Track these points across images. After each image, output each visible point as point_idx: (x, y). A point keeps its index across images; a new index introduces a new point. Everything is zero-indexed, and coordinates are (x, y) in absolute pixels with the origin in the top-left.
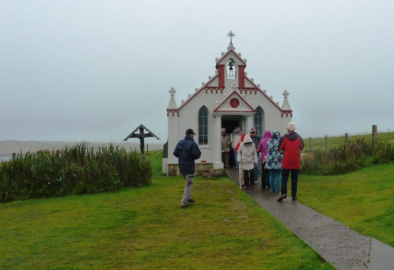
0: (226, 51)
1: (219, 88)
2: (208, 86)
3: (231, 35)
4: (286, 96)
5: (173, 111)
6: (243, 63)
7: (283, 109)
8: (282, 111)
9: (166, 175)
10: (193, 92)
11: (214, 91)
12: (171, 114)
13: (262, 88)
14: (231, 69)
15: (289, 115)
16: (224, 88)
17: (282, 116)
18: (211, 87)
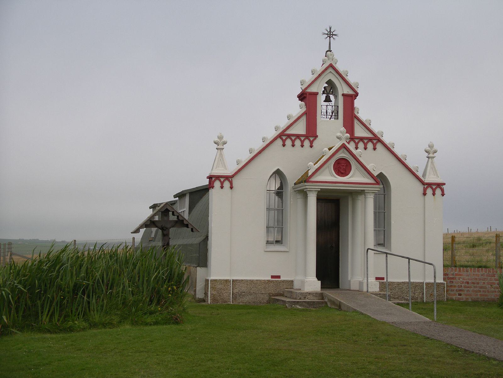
1: (307, 137)
2: (288, 132)
3: (330, 34)
4: (431, 155)
5: (222, 180)
7: (425, 182)
9: (204, 301)
10: (258, 145)
11: (298, 143)
13: (386, 139)
14: (328, 100)
15: (438, 191)
16: (317, 137)
17: (425, 194)
18: (293, 135)
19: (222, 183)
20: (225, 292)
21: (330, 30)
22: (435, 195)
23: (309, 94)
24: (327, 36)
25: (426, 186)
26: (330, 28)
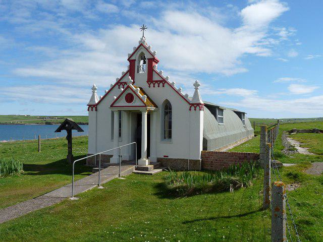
0: (137, 45)
2: (121, 81)
6: (153, 56)
8: (190, 104)
12: (90, 108)
13: (170, 81)
14: (145, 63)
15: (198, 108)
17: (190, 110)
18: (124, 83)
19: (92, 108)
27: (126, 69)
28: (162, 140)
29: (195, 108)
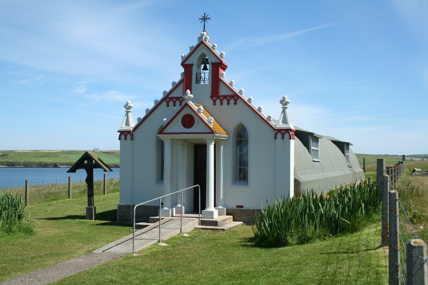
0: (195, 43)
2: (171, 96)
7: (276, 128)
10: (151, 106)
12: (123, 136)
17: (275, 138)
19: (126, 136)
20: (127, 214)
21: (205, 16)
22: (284, 139)
23: (186, 66)
24: (202, 20)
25: (276, 132)
26: (205, 14)
27: (178, 78)
28: (232, 185)
29: (283, 135)
